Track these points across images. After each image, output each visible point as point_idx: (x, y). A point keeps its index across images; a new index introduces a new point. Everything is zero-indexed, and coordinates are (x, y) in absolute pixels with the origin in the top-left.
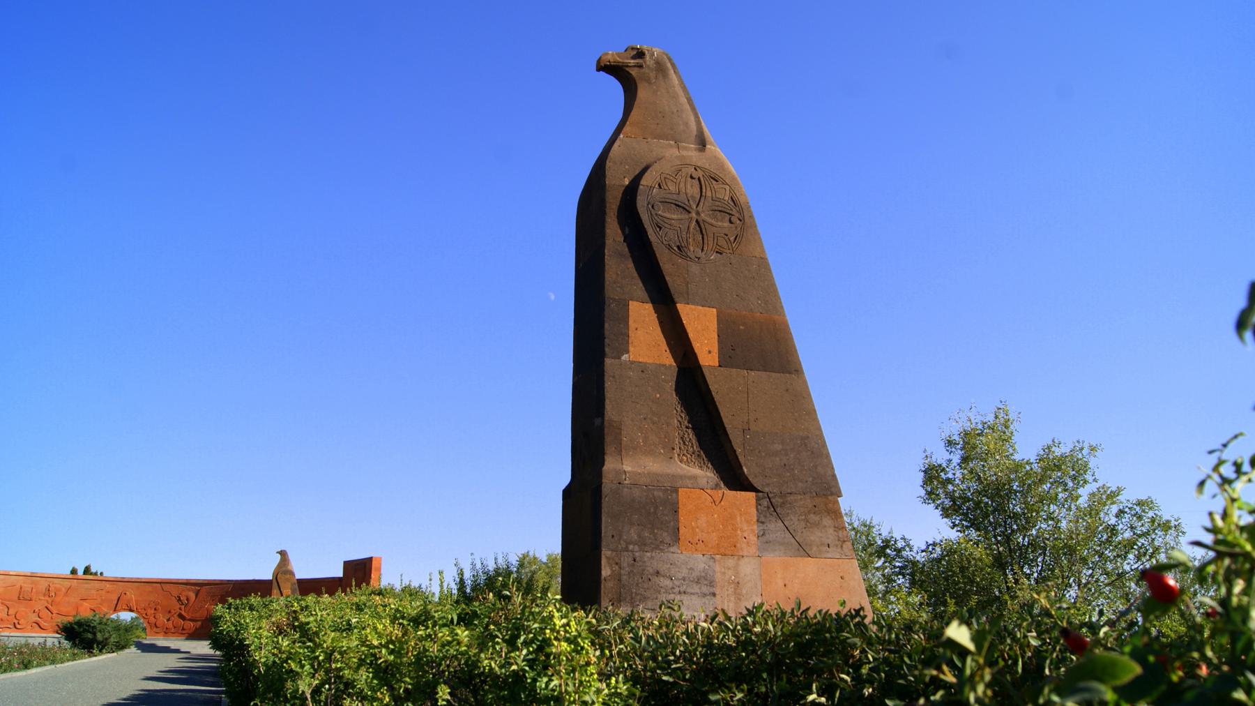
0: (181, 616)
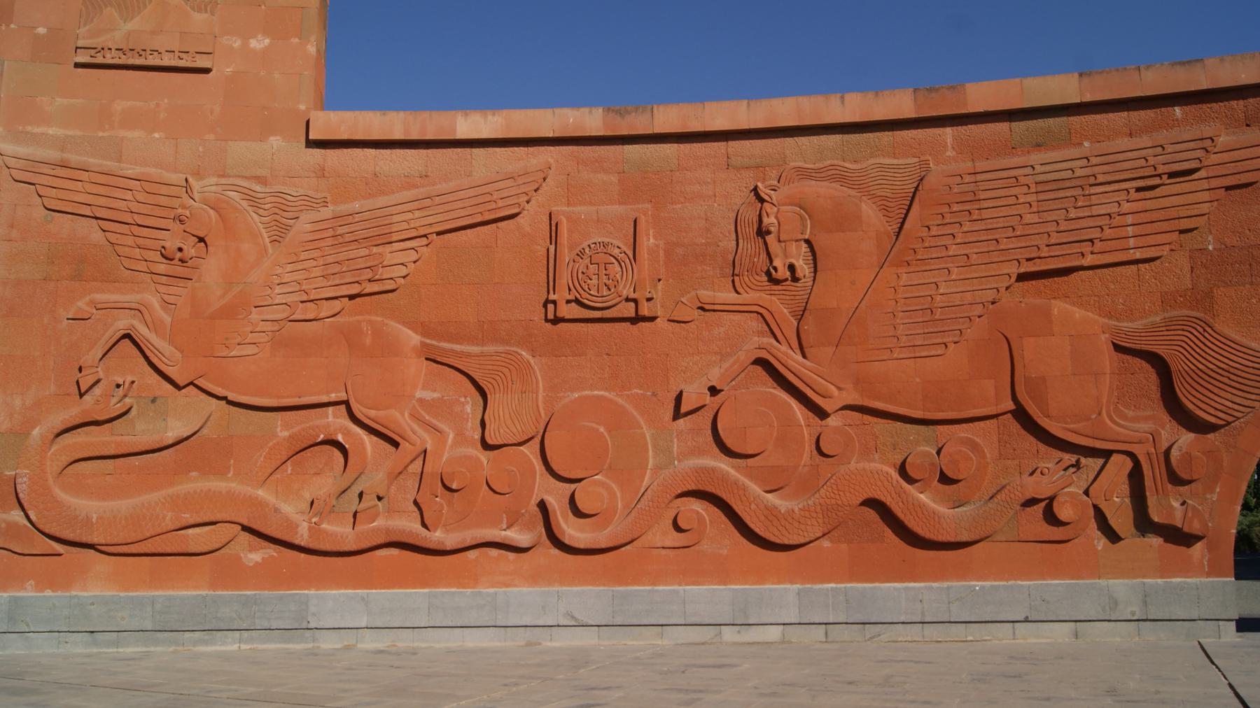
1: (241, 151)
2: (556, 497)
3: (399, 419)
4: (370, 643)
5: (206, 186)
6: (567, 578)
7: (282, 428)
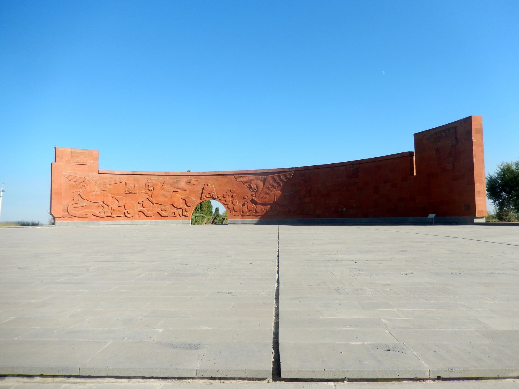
0: (253, 201)
1: (91, 174)
2: (126, 212)
3: (109, 204)
4: (106, 226)
5: (87, 178)
6: (126, 220)
7: (96, 204)
